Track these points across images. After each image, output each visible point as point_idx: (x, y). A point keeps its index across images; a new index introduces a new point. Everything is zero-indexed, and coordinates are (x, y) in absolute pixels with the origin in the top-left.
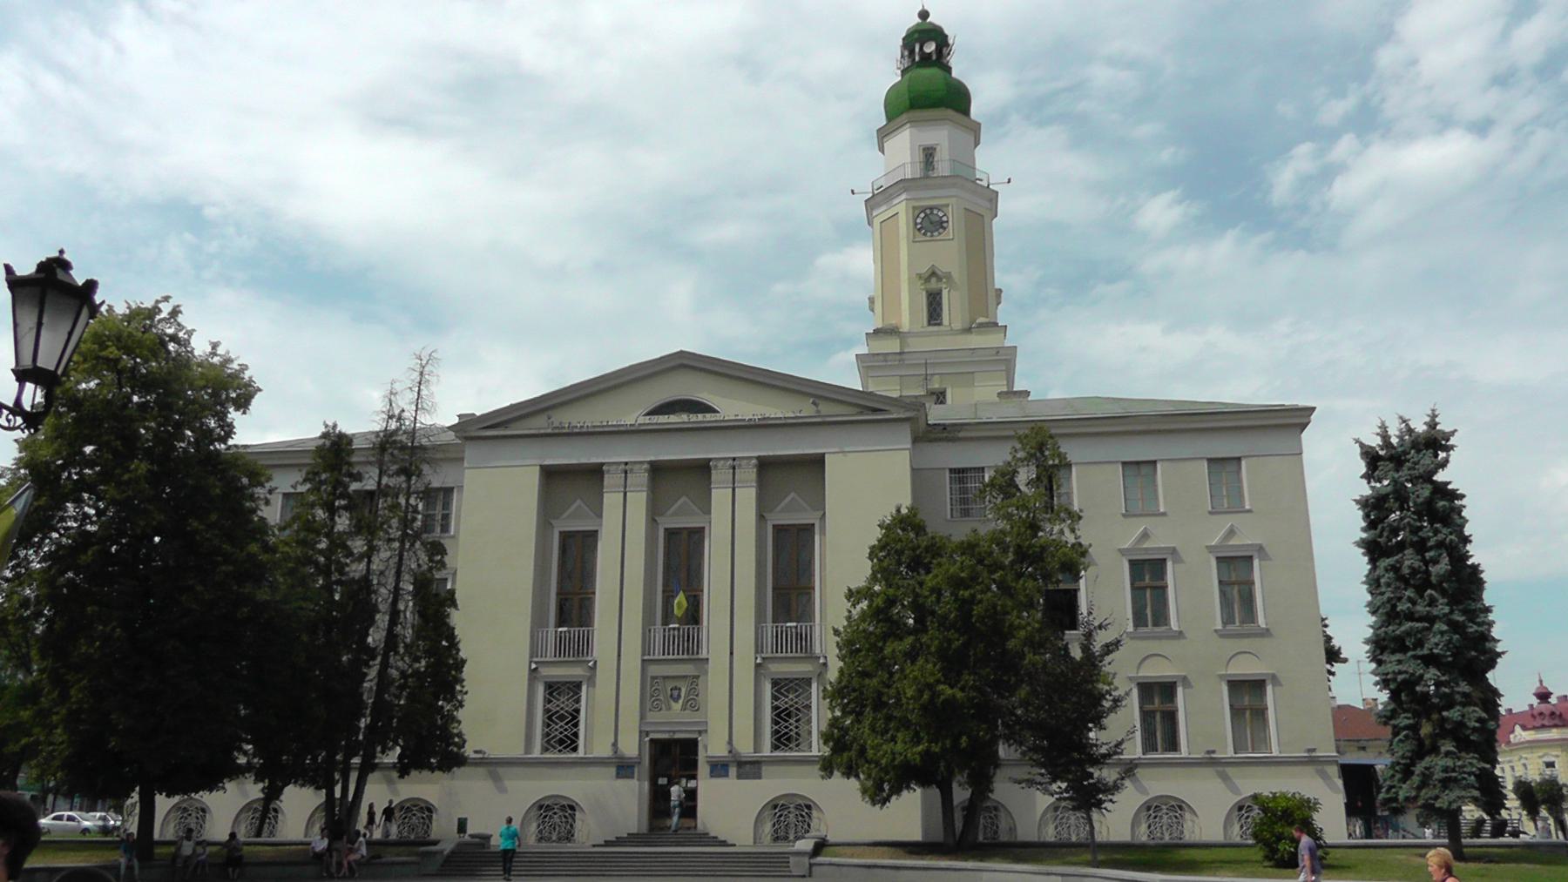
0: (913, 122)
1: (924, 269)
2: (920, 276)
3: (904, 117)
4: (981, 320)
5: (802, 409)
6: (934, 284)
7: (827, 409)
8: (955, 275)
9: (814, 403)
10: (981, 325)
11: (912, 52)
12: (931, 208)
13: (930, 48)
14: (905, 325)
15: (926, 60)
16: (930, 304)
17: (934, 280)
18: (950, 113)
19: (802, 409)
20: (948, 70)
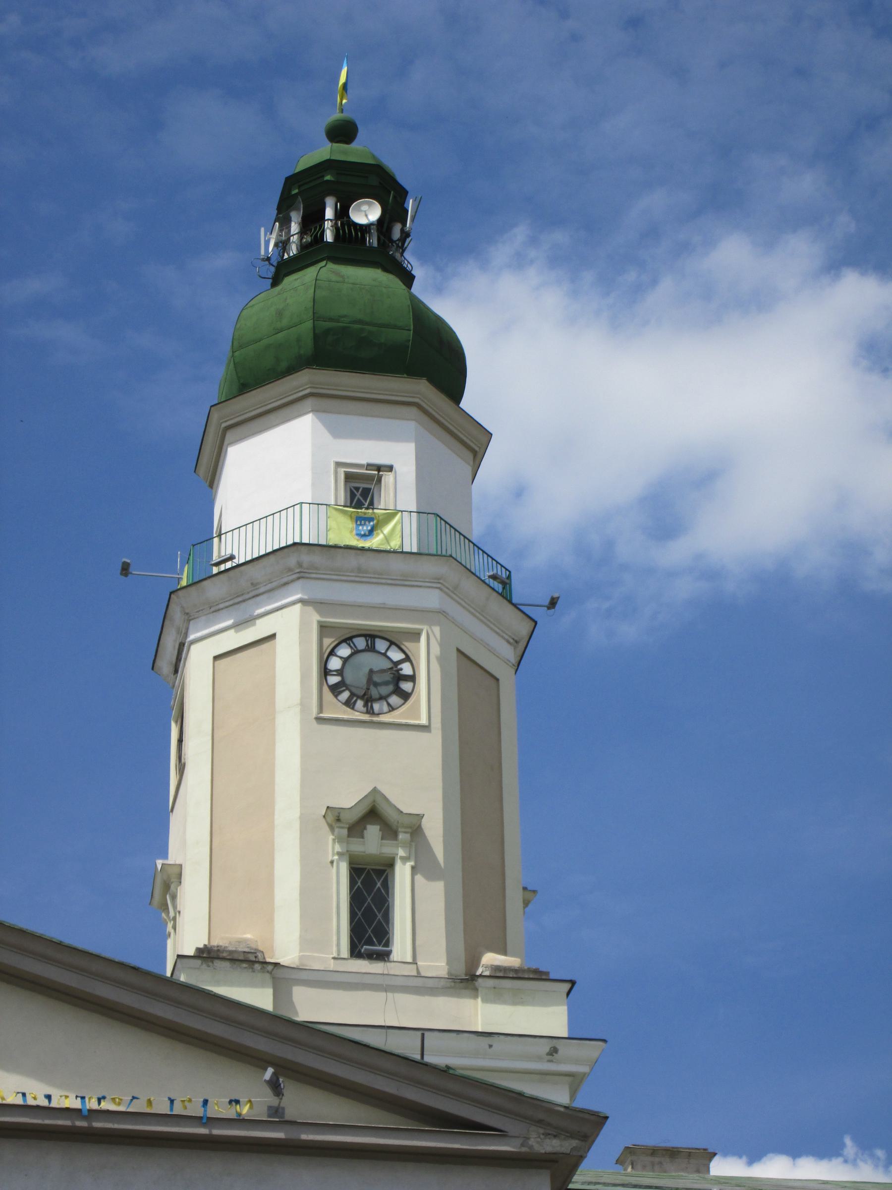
0: (322, 400)
1: (349, 797)
2: (334, 817)
3: (304, 379)
4: (490, 959)
5: (230, 1095)
6: (372, 843)
7: (306, 1105)
8: (434, 829)
9: (275, 1086)
10: (500, 973)
11: (312, 220)
12: (371, 636)
13: (367, 213)
14: (286, 949)
15: (352, 245)
16: (356, 899)
17: (373, 831)
18: (422, 388)
19: (230, 1095)
20: (408, 278)
